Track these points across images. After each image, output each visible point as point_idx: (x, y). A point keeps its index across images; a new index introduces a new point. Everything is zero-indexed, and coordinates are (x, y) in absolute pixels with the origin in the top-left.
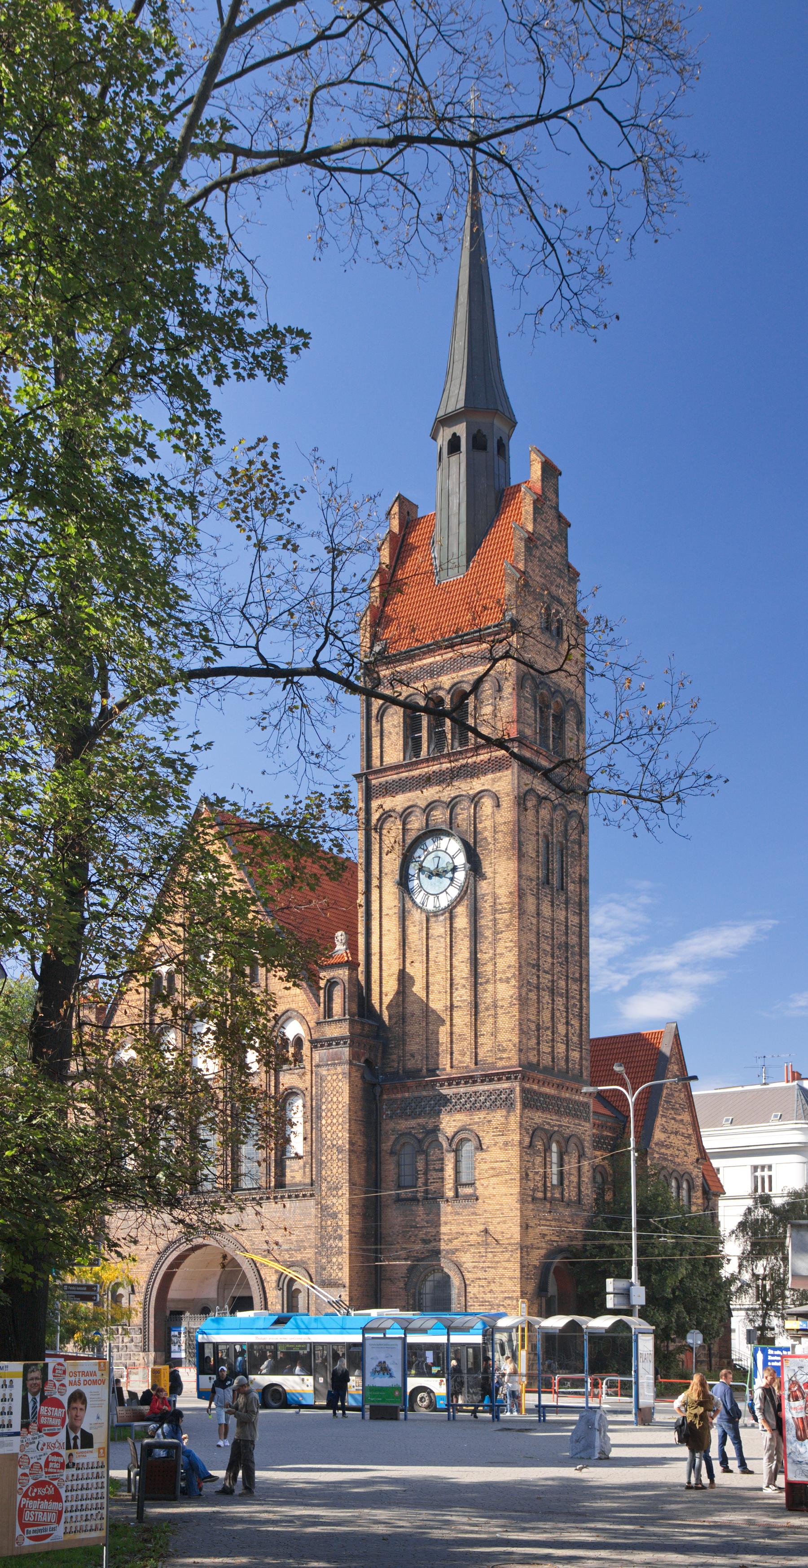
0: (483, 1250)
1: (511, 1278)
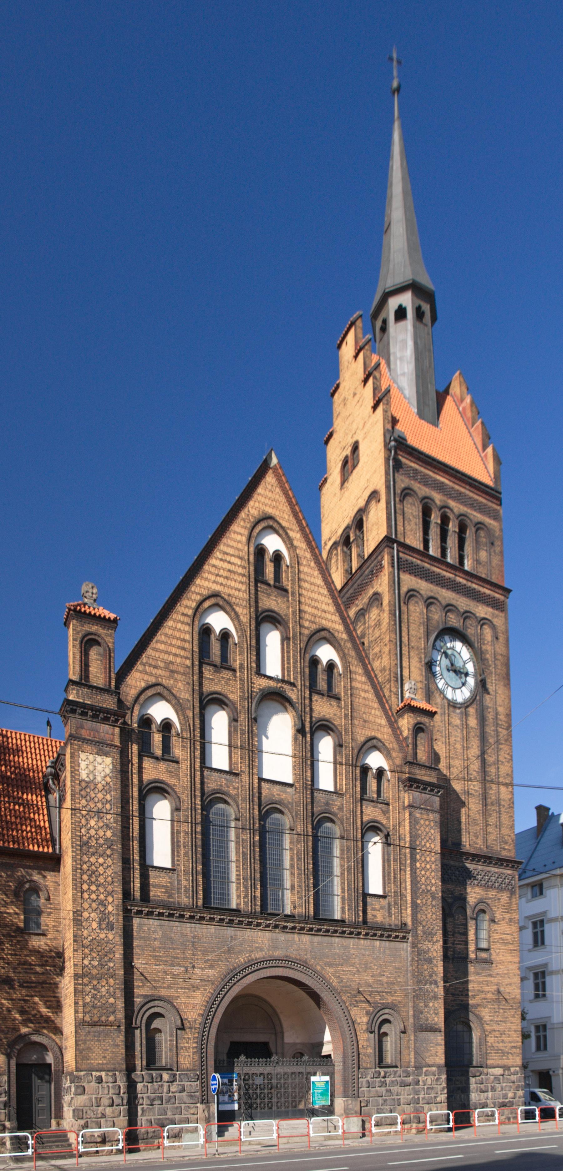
0: (496, 1007)
1: (515, 1031)
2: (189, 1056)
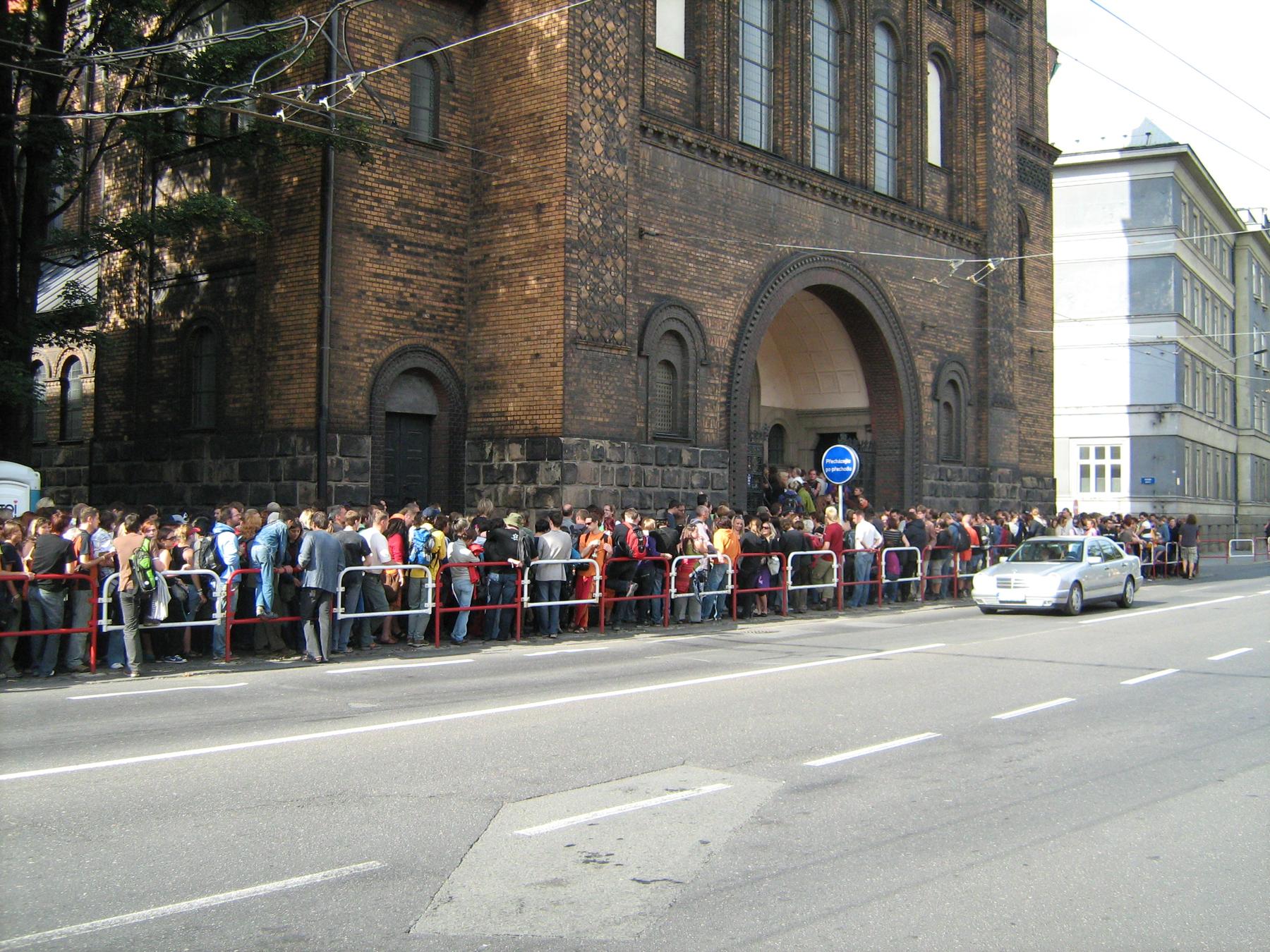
2: (715, 418)
